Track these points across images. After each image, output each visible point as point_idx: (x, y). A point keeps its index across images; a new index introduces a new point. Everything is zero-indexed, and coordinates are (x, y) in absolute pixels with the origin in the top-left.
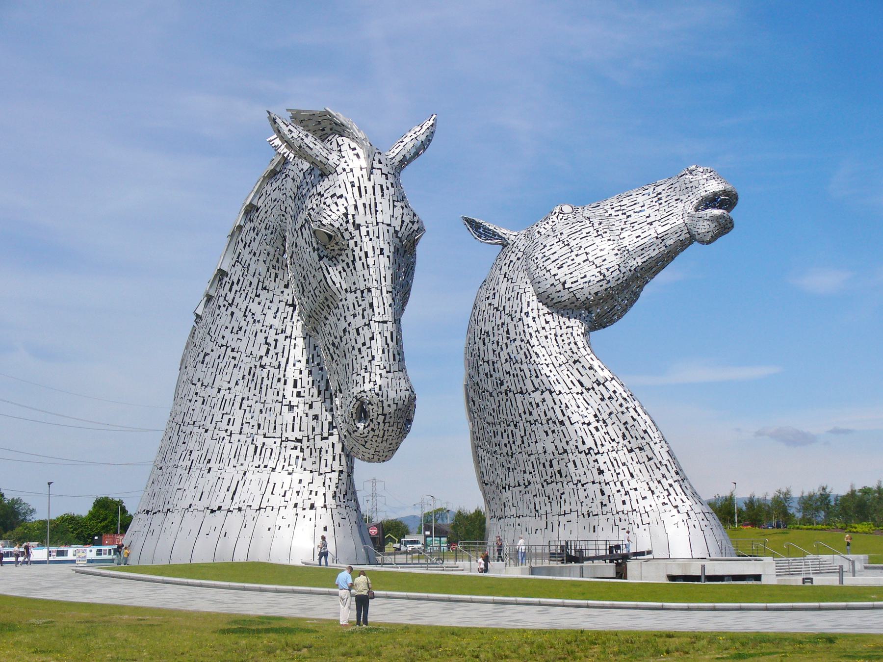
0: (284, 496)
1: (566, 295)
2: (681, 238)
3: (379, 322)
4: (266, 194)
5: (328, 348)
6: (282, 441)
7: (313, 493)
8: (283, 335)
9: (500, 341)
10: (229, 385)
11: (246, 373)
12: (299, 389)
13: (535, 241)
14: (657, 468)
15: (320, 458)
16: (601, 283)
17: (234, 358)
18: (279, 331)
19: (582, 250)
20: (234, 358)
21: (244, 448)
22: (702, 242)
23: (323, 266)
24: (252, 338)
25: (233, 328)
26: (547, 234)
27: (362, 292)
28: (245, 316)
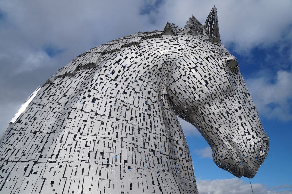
4: (148, 43)
5: (222, 114)
6: (170, 158)
10: (126, 119)
11: (138, 115)
17: (126, 106)
20: (126, 106)
21: (150, 158)
24: (136, 100)
25: (119, 91)
27: (246, 94)
28: (127, 87)
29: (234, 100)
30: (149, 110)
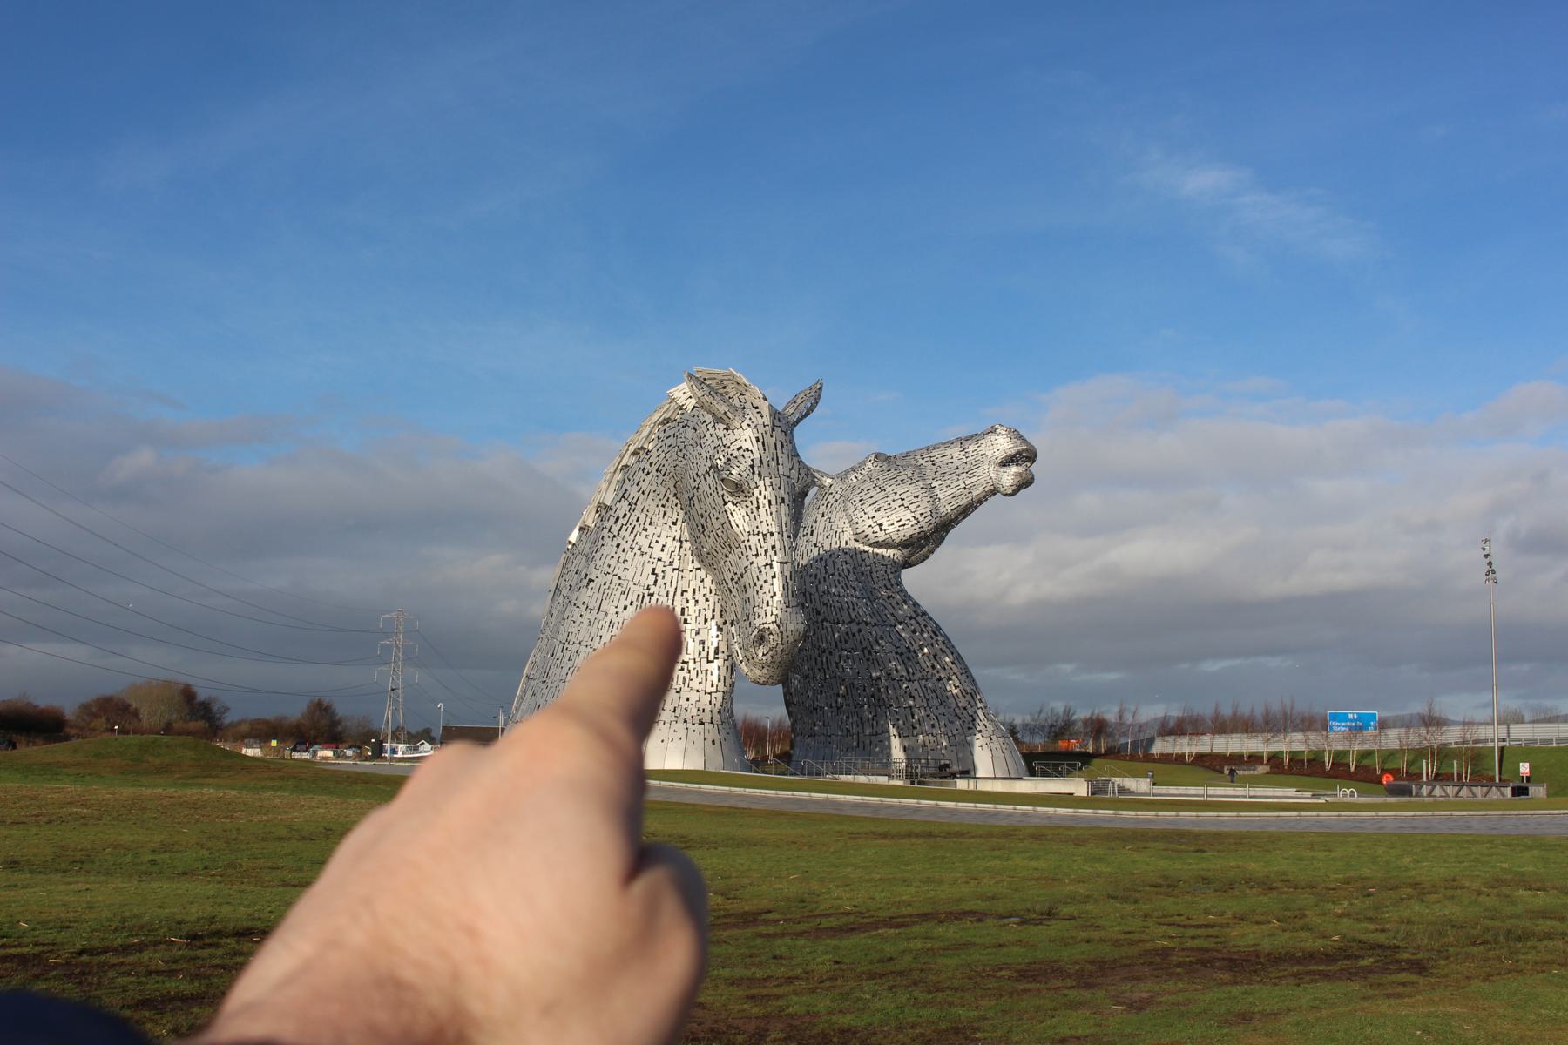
0: (674, 711)
1: (882, 536)
2: (987, 489)
3: (781, 563)
5: (727, 584)
7: (701, 710)
8: (672, 567)
9: (819, 575)
10: (616, 610)
11: (634, 599)
12: (686, 616)
13: (852, 485)
14: (963, 695)
15: (706, 680)
16: (915, 527)
18: (667, 563)
19: (897, 497)
22: (1005, 495)
23: (727, 510)
26: (864, 478)
27: (764, 535)
29: (740, 555)
30: (656, 582)
